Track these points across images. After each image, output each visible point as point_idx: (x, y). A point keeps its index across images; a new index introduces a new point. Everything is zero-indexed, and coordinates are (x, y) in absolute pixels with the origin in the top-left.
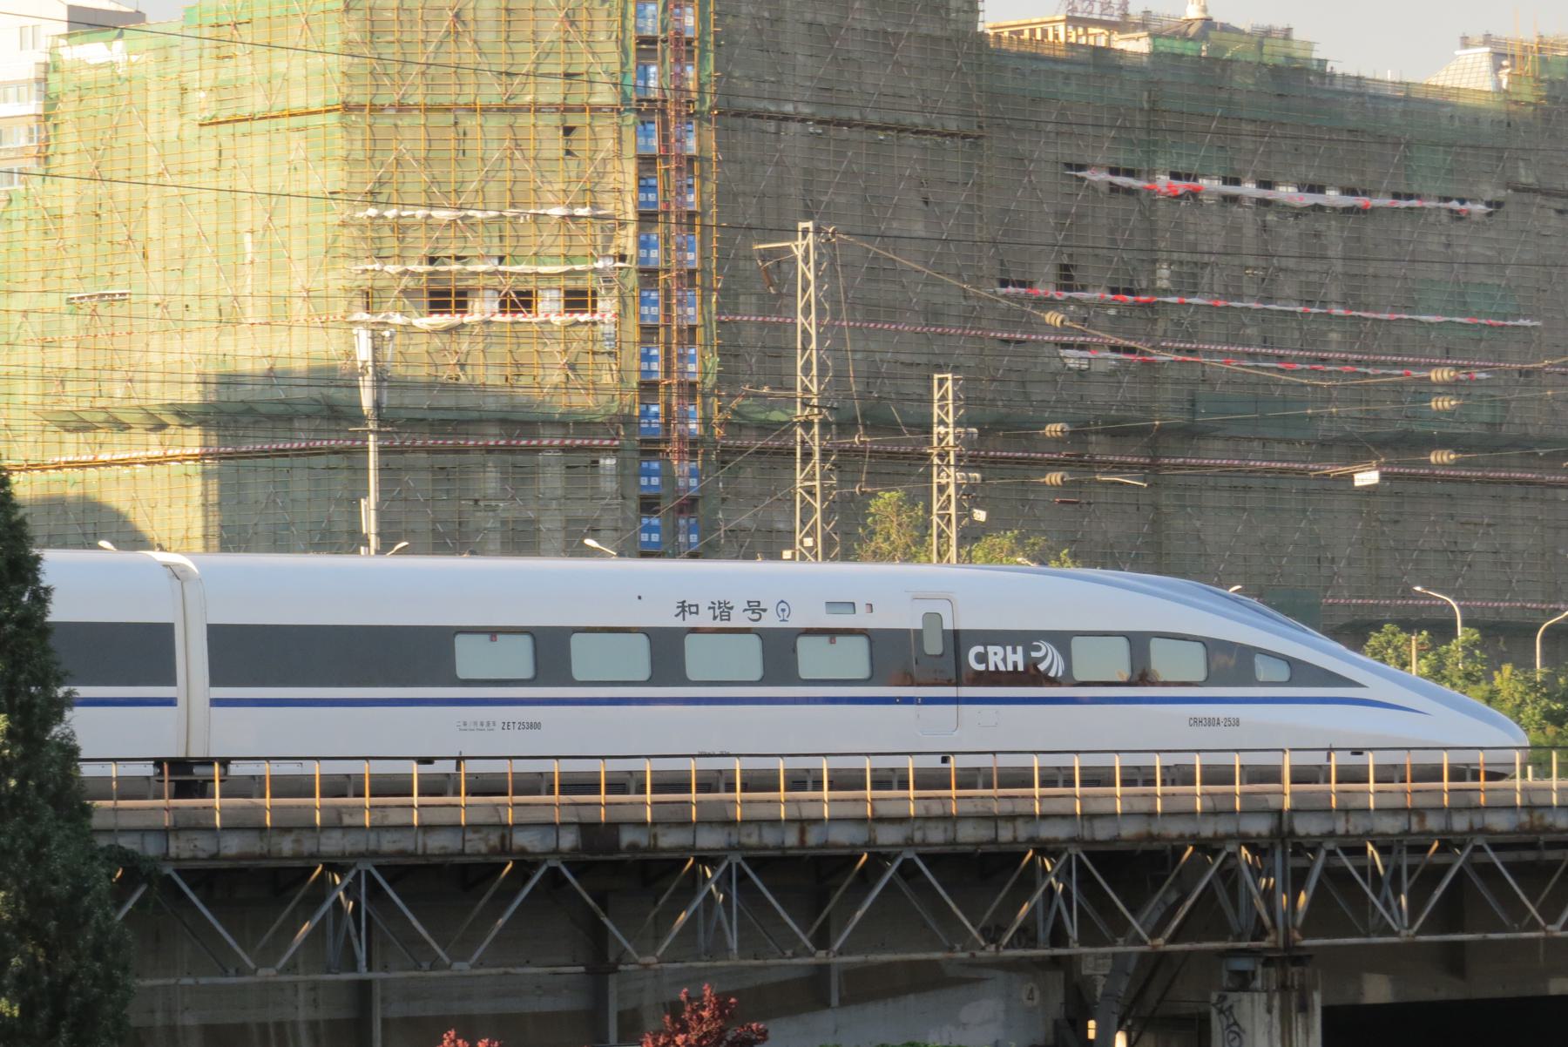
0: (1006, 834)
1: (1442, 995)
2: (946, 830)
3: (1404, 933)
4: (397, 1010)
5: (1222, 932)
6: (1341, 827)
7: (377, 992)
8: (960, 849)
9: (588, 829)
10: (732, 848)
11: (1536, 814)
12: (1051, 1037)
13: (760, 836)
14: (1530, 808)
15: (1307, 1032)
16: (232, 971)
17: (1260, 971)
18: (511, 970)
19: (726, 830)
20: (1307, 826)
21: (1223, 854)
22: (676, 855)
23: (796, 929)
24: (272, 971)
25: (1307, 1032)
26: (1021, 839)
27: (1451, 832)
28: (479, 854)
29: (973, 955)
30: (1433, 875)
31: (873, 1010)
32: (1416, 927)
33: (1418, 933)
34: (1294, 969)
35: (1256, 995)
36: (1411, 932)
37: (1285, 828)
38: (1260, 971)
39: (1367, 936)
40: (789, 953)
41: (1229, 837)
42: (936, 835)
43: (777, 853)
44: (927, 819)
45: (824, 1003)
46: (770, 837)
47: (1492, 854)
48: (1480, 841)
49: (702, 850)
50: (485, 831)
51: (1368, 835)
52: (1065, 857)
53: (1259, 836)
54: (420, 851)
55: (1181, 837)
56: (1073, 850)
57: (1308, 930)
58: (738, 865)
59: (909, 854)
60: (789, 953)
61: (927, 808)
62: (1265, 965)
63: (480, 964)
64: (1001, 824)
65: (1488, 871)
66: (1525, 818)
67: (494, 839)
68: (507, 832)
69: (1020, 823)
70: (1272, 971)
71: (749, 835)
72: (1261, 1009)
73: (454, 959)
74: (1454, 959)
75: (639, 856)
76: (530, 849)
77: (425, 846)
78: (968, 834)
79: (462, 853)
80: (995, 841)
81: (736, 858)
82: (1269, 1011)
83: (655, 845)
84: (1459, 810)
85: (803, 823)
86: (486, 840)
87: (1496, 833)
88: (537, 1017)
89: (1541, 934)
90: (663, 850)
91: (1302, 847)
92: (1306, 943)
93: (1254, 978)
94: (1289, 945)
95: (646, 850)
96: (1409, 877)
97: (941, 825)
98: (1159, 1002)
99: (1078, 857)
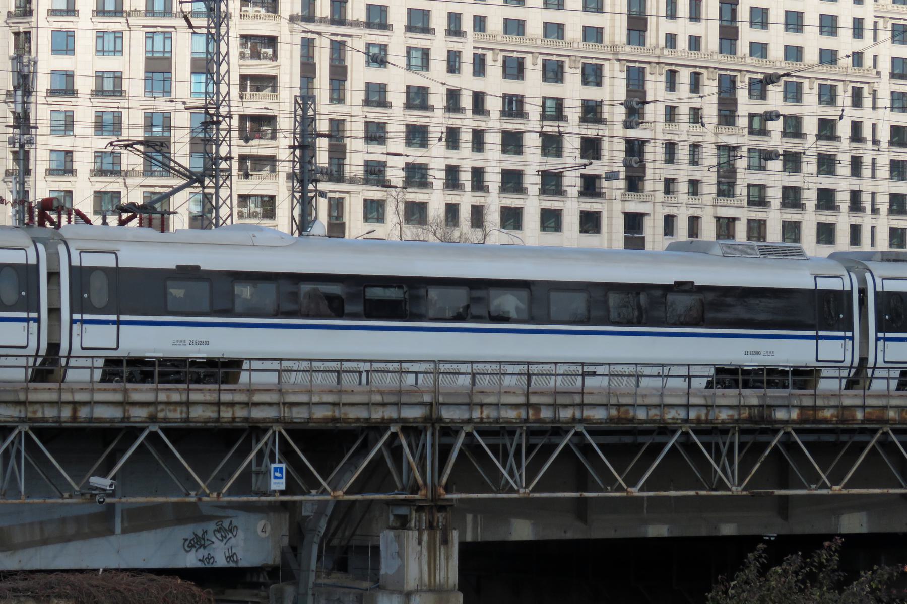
0: (226, 414)
1: (569, 535)
2: (181, 413)
3: (522, 491)
5: (389, 487)
6: (476, 415)
10: (22, 420)
11: (622, 409)
12: (278, 561)
13: (43, 413)
14: (619, 406)
15: (448, 558)
17: (414, 514)
19: (18, 408)
20: (448, 414)
21: (389, 433)
23: (68, 478)
25: (448, 558)
26: (237, 420)
27: (559, 421)
29: (200, 499)
30: (548, 450)
32: (530, 488)
33: (533, 491)
34: (439, 515)
35: (410, 532)
36: (527, 491)
37: (434, 416)
39: (498, 492)
40: (66, 495)
41: (392, 421)
42: (176, 414)
44: (168, 403)
45: (112, 532)
46: (50, 413)
47: (588, 437)
48: (580, 428)
51: (497, 421)
52: (271, 432)
53: (415, 420)
55: (358, 420)
56: (277, 428)
57: (448, 489)
58: (26, 434)
59: (154, 428)
60: (66, 495)
61: (168, 397)
62: (417, 511)
64: (222, 408)
65: (587, 449)
66: (614, 412)
69: (237, 408)
70: (424, 518)
71: (35, 412)
74: (581, 509)
78: (197, 413)
80: (218, 420)
82: (420, 543)
84: (566, 406)
85: (75, 404)
87: (593, 423)
89: (624, 494)
91: (449, 431)
92: (449, 496)
93: (410, 521)
94: (435, 498)
96: (528, 452)
97: (179, 409)
98: (353, 534)
99: (280, 433)
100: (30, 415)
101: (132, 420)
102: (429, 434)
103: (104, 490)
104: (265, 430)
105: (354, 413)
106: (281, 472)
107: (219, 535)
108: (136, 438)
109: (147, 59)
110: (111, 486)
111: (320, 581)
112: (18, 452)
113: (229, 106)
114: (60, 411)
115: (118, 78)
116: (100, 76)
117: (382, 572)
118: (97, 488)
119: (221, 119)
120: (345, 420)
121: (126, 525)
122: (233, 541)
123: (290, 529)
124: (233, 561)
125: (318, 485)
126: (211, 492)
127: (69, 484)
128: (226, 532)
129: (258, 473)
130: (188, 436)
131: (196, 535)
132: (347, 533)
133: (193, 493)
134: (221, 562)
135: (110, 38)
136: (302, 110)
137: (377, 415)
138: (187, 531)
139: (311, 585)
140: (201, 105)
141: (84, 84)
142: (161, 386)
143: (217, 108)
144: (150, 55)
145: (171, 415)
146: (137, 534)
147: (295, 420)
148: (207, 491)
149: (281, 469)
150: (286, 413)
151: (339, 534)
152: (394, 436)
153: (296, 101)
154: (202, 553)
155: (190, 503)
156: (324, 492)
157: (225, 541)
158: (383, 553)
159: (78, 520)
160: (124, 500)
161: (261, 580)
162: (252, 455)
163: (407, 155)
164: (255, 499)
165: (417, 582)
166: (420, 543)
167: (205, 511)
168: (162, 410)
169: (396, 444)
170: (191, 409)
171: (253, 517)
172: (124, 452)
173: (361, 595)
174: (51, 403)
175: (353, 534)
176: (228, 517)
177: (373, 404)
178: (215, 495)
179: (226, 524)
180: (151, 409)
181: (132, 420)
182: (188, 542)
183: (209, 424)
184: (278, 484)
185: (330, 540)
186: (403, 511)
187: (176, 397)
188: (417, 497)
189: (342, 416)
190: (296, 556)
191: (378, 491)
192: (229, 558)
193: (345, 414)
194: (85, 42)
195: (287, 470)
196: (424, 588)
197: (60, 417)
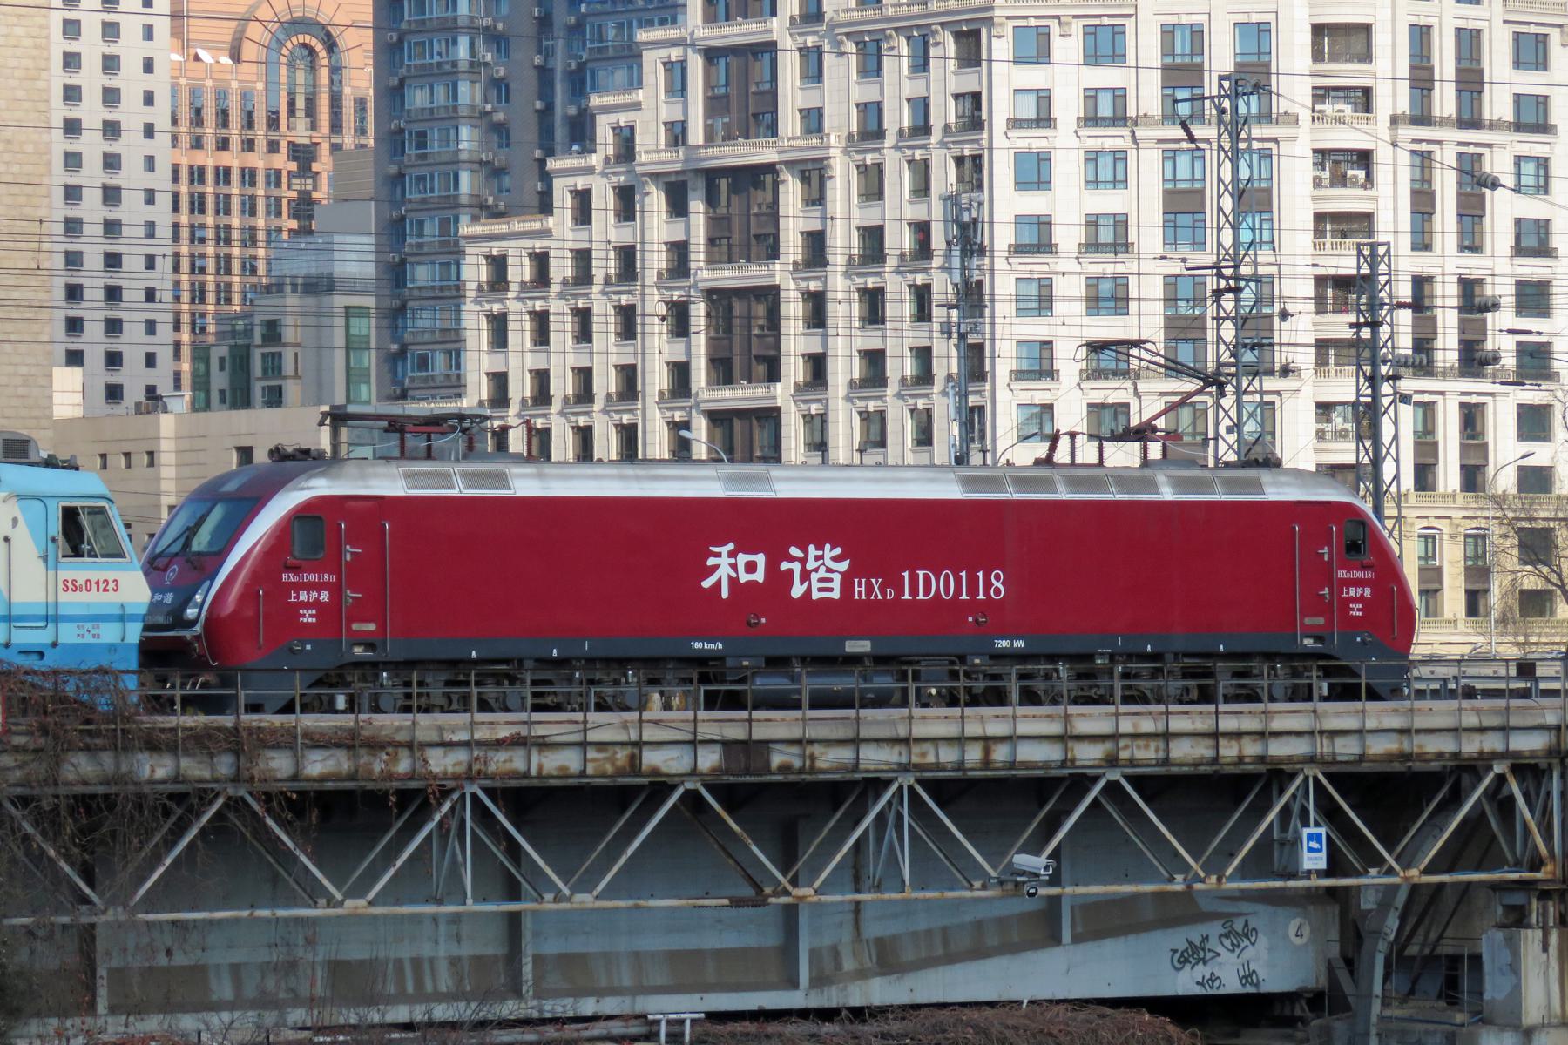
0: (1229, 751)
2: (1157, 751)
4: (551, 947)
7: (527, 925)
8: (1175, 770)
9: (727, 744)
10: (905, 768)
12: (1323, 982)
13: (937, 755)
16: (322, 902)
17: (1535, 904)
18: (642, 903)
19: (897, 749)
21: (1491, 776)
22: (837, 777)
24: (362, 902)
28: (604, 776)
29: (1189, 887)
31: (1111, 948)
35: (1529, 932)
38: (1535, 904)
40: (977, 884)
43: (959, 774)
44: (1136, 736)
45: (1053, 939)
46: (948, 755)
49: (867, 771)
50: (611, 749)
52: (1300, 778)
54: (534, 772)
55: (1440, 755)
56: (1311, 771)
58: (911, 788)
59: (1115, 775)
60: (977, 884)
61: (1135, 726)
62: (1539, 899)
63: (611, 892)
64: (1222, 742)
67: (622, 755)
68: (636, 751)
69: (1246, 741)
71: (923, 755)
72: (1537, 947)
73: (574, 890)
75: (792, 778)
76: (665, 769)
77: (540, 767)
78: (1182, 750)
79: (583, 774)
80: (1215, 760)
81: (908, 780)
82: (1545, 949)
83: (812, 767)
85: (987, 741)
86: (612, 760)
88: (720, 955)
90: (822, 771)
95: (801, 771)
97: (1153, 745)
98: (1440, 937)
99: (1316, 779)
100: (915, 760)
101: (1078, 763)
102: (1556, 775)
103: (1037, 875)
104: (1293, 776)
105: (1433, 745)
106: (1319, 841)
107: (1227, 943)
108: (1087, 791)
109: (1166, 192)
110: (1046, 868)
111: (1387, 1013)
112: (900, 817)
113: (1256, 264)
114: (963, 752)
115: (1121, 223)
116: (1092, 222)
117: (1487, 996)
118: (1024, 873)
119: (1242, 284)
120: (1421, 757)
121: (1079, 929)
122: (1250, 953)
123: (1342, 932)
124: (1252, 983)
125: (1378, 861)
126: (1208, 875)
127: (982, 867)
128: (1239, 937)
129: (1282, 844)
130: (1165, 787)
131: (1191, 943)
132: (1433, 936)
133: (1179, 878)
134: (1231, 985)
135: (1105, 163)
136: (1370, 266)
137: (1471, 746)
138: (1178, 938)
139: (1374, 1019)
140: (1210, 263)
141: (1068, 236)
142: (1123, 709)
143: (1236, 267)
144: (1169, 186)
145: (1140, 754)
146: (1096, 944)
147: (1339, 758)
148: (1202, 874)
149: (1319, 835)
150: (1324, 747)
151: (1419, 938)
152: (1501, 779)
153: (1360, 253)
154: (1201, 971)
155: (1175, 893)
156: (1390, 871)
157: (1237, 951)
158: (1487, 967)
159: (1001, 922)
160: (1069, 890)
161: (1298, 1012)
162: (1272, 815)
163: (1540, 333)
164: (1278, 884)
165: (1543, 1012)
166: (1545, 949)
167: (1206, 905)
168: (1126, 747)
169: (1505, 792)
170: (1171, 745)
171: (1281, 912)
172: (1069, 813)
173: (1453, 1034)
174: (949, 740)
175: (1440, 937)
176: (1239, 915)
177: (1466, 730)
178: (1214, 879)
179: (1238, 925)
180: (1108, 746)
181: (1078, 763)
182: (1177, 955)
183: (1202, 768)
184: (1314, 860)
185: (1404, 947)
186: (1517, 899)
187: (1147, 726)
188: (1539, 875)
189: (1416, 750)
190: (1352, 973)
191: (1478, 868)
192: (1246, 979)
193: (1420, 747)
194: (1067, 168)
195: (1328, 837)
196: (1554, 1021)
197: (962, 762)
